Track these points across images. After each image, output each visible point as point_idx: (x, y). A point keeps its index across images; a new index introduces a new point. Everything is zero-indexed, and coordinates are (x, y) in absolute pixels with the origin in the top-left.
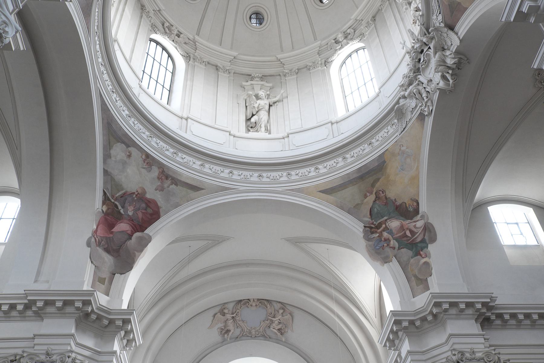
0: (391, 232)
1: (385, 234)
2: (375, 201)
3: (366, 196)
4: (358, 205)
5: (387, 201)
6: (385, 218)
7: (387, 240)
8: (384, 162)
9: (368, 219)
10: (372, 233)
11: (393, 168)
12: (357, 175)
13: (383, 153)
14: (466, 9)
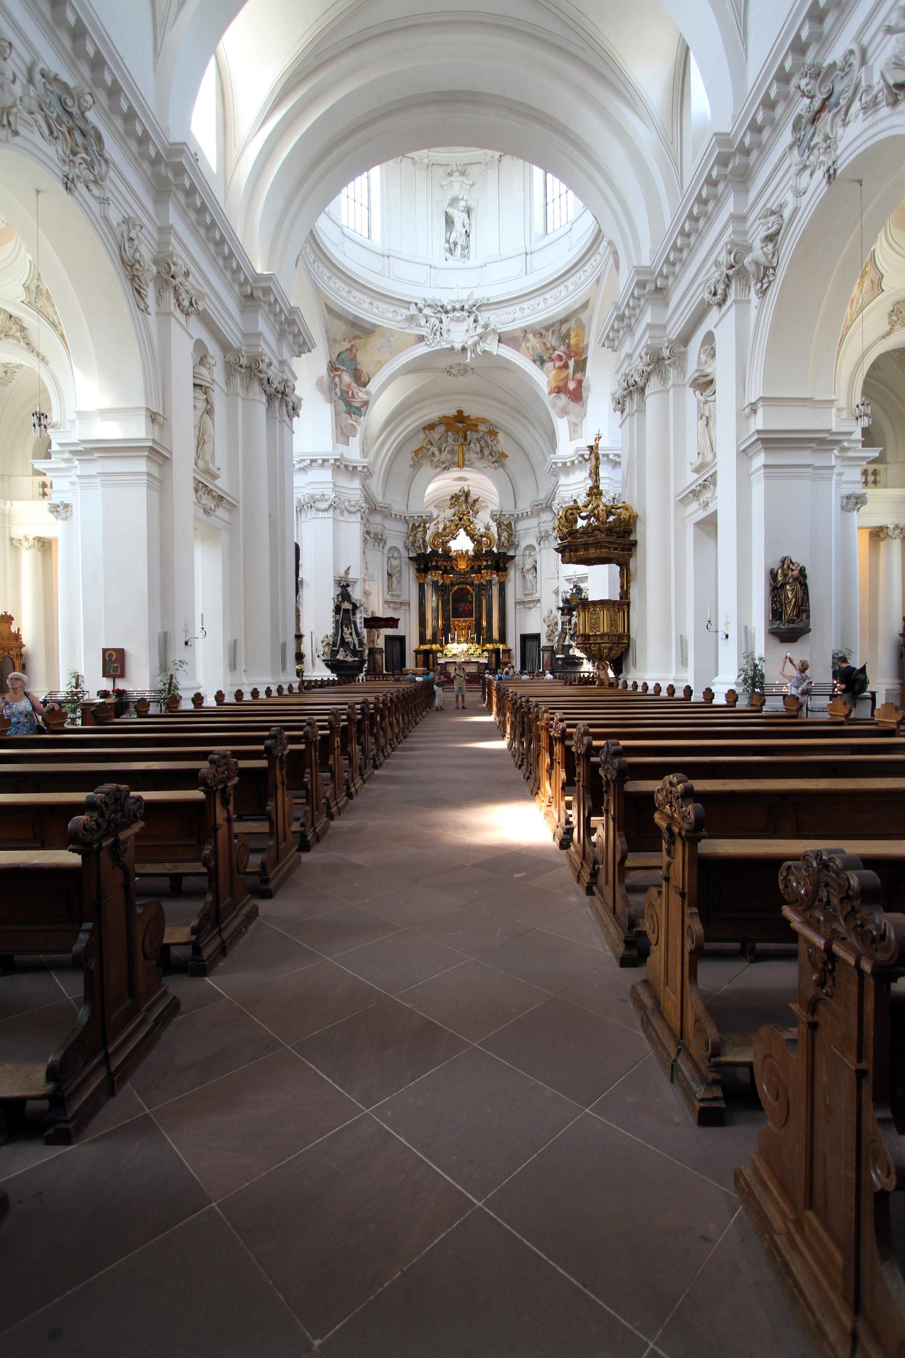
0: (341, 382)
1: (337, 379)
2: (347, 350)
3: (345, 340)
4: (336, 340)
5: (354, 359)
6: (344, 368)
7: (335, 385)
8: (374, 332)
9: (334, 357)
10: (332, 371)
11: (374, 341)
12: (353, 320)
13: (378, 326)
14: (518, 351)
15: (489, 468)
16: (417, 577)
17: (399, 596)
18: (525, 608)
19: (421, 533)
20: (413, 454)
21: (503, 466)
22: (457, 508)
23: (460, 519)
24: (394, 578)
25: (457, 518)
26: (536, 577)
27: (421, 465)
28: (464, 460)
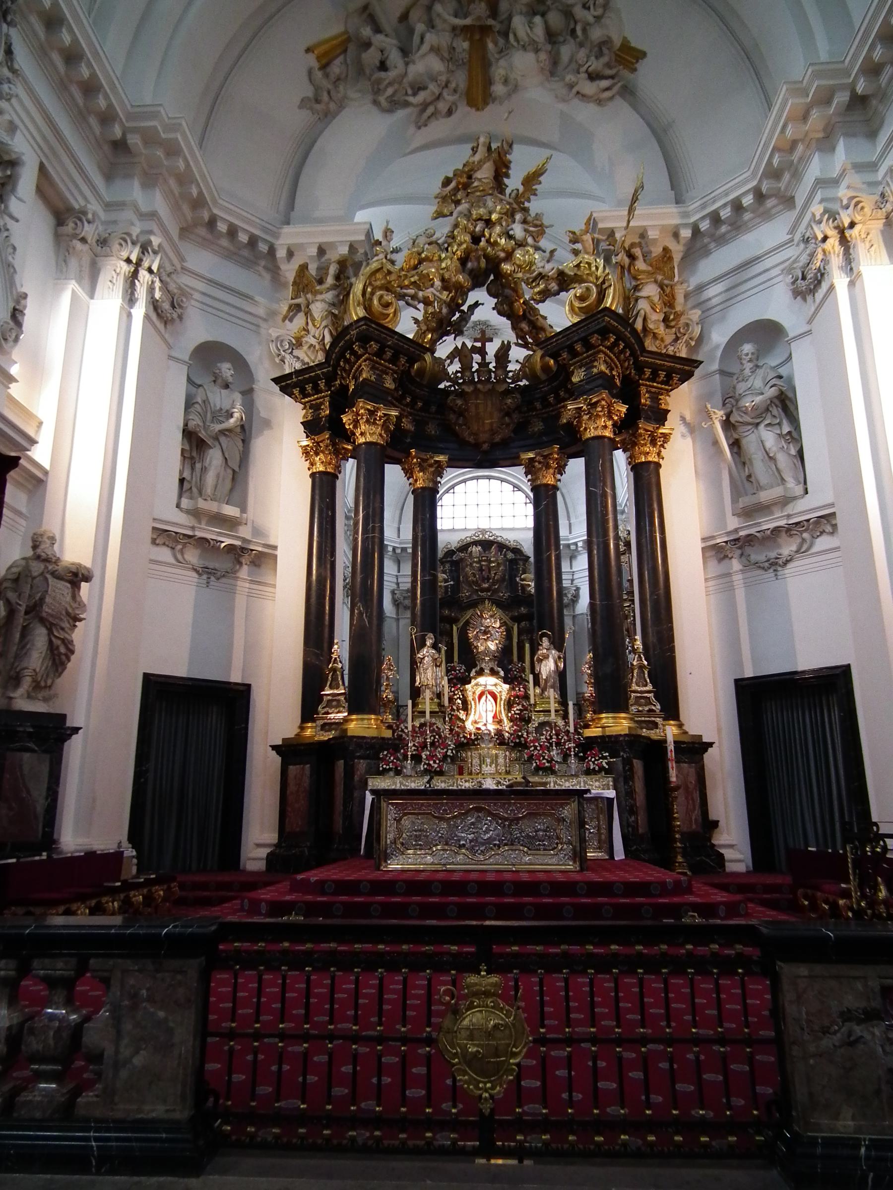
15: (576, 102)
16: (306, 452)
17: (231, 524)
18: (757, 565)
19: (329, 296)
20: (311, 60)
21: (628, 92)
22: (464, 207)
23: (476, 239)
24: (214, 458)
25: (468, 238)
26: (794, 437)
27: (341, 107)
28: (488, 82)
